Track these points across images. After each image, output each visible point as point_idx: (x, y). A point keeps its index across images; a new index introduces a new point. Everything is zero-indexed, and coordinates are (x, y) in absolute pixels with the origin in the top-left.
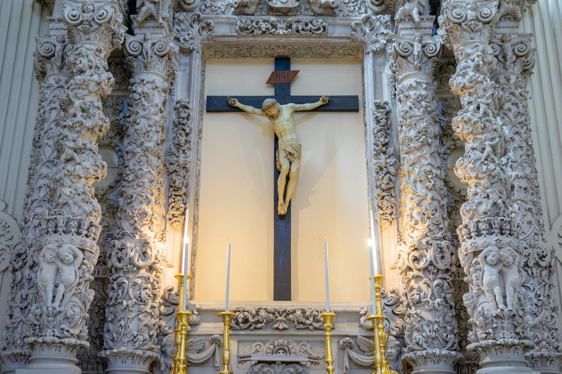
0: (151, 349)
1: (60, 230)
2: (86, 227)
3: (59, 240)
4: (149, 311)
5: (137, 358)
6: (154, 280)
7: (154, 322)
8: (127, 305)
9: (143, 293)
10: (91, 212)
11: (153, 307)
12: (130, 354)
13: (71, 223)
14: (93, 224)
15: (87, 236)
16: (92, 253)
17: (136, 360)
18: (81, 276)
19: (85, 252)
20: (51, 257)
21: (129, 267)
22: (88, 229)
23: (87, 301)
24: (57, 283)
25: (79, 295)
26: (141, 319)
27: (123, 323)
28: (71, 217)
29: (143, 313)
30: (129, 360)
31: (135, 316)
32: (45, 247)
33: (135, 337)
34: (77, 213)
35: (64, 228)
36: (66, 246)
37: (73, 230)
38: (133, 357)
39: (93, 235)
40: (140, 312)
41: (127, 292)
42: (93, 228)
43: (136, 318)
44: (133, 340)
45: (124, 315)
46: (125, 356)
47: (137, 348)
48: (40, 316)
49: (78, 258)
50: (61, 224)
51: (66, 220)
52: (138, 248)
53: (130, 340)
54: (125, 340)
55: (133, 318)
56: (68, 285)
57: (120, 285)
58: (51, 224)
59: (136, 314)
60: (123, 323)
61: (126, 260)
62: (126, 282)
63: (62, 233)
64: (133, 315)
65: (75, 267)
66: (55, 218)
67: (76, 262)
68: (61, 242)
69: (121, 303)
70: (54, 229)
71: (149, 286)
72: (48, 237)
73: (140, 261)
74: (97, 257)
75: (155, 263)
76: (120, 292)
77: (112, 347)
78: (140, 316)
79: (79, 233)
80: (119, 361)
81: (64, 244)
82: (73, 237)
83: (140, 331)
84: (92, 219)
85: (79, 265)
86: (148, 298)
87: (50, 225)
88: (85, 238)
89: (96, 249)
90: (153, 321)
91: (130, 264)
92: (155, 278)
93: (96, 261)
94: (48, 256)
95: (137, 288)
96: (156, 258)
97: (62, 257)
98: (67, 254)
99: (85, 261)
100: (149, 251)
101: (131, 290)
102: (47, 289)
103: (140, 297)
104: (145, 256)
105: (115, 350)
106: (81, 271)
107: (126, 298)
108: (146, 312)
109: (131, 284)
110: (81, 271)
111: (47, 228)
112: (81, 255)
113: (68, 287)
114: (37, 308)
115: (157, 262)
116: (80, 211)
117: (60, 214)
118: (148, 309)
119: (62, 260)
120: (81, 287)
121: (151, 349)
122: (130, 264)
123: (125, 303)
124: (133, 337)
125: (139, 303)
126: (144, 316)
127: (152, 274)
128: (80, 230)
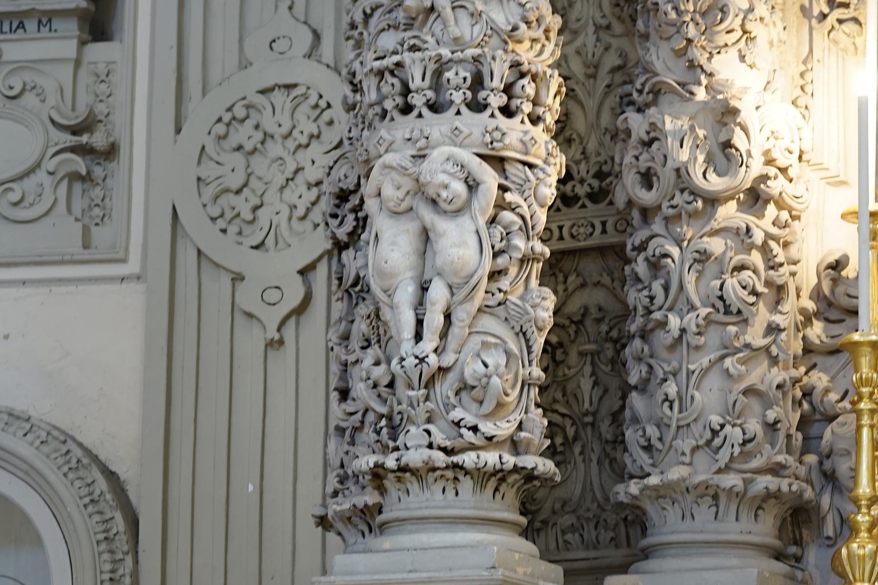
0: (776, 470)
1: (417, 100)
2: (497, 83)
3: (416, 133)
4: (759, 342)
5: (729, 498)
6: (768, 236)
7: (778, 380)
8: (683, 331)
9: (732, 283)
10: (515, 29)
11: (773, 329)
12: (701, 490)
13: (449, 75)
14: (525, 68)
15: (508, 111)
16: (531, 166)
17: (728, 507)
18: (498, 246)
19: (507, 166)
20: (400, 194)
21: (678, 200)
22: (508, 89)
23: (531, 330)
24: (426, 277)
25: (500, 310)
26: (732, 370)
27: (671, 389)
28: (446, 53)
29: (739, 350)
30: (704, 507)
31: (712, 364)
32: (378, 164)
33: (715, 433)
34: (467, 37)
35: (430, 94)
36: (437, 155)
37: (458, 97)
38: (715, 497)
39: (527, 108)
40: (728, 350)
41: (681, 287)
42: (525, 81)
43: (716, 369)
44: (709, 443)
45: (675, 364)
46: (690, 498)
47: (726, 469)
48: (391, 385)
49: (481, 187)
50: (416, 83)
51: (432, 67)
52: (701, 133)
53: (701, 442)
54: (685, 444)
55: (705, 372)
56: (455, 280)
57: (656, 265)
58: (391, 85)
59: (713, 356)
60: (671, 389)
61: (666, 176)
62: (675, 251)
63: (425, 111)
64: (705, 362)
65: (474, 219)
66: (399, 65)
67: (476, 205)
68: (422, 143)
69: (663, 324)
70: (399, 100)
71: (756, 258)
72: (384, 131)
73: (712, 176)
74: (553, 180)
75: (764, 178)
76: (657, 287)
77: (647, 469)
78: (728, 362)
79: (477, 106)
80: (673, 514)
81: (434, 148)
82: (458, 122)
83: (733, 414)
84: (525, 53)
85: (491, 211)
86: (752, 299)
87: (386, 89)
88: (502, 121)
89: (543, 154)
90: (778, 375)
91: (682, 191)
92: (774, 231)
93: (549, 193)
94: (388, 191)
95: (711, 268)
96: (769, 162)
97: (431, 192)
98: (443, 178)
99: (509, 197)
100: (739, 139)
101: (690, 280)
102: (396, 299)
103: (721, 298)
104: (728, 158)
105: (654, 480)
106: (498, 231)
107: (679, 305)
108: (747, 346)
109: (690, 257)
110: (498, 231)
111: (380, 103)
112: (490, 178)
113: (460, 287)
114: (377, 363)
115: (772, 171)
116: (477, 28)
117: (413, 49)
118: (755, 336)
119: (434, 202)
120: (504, 283)
121: (776, 470)
122: (682, 191)
123: (674, 321)
124: (708, 435)
125: (721, 317)
126: (743, 362)
127: (761, 216)
128: (482, 95)
